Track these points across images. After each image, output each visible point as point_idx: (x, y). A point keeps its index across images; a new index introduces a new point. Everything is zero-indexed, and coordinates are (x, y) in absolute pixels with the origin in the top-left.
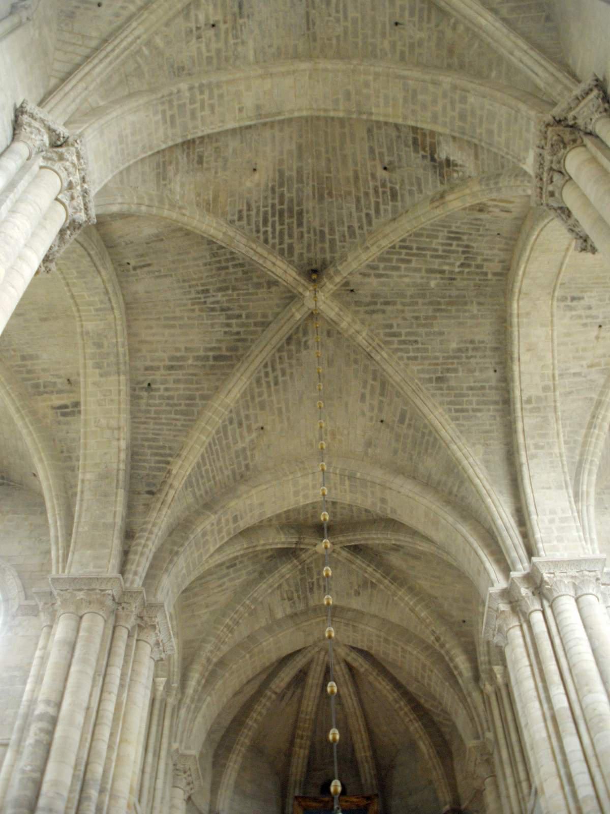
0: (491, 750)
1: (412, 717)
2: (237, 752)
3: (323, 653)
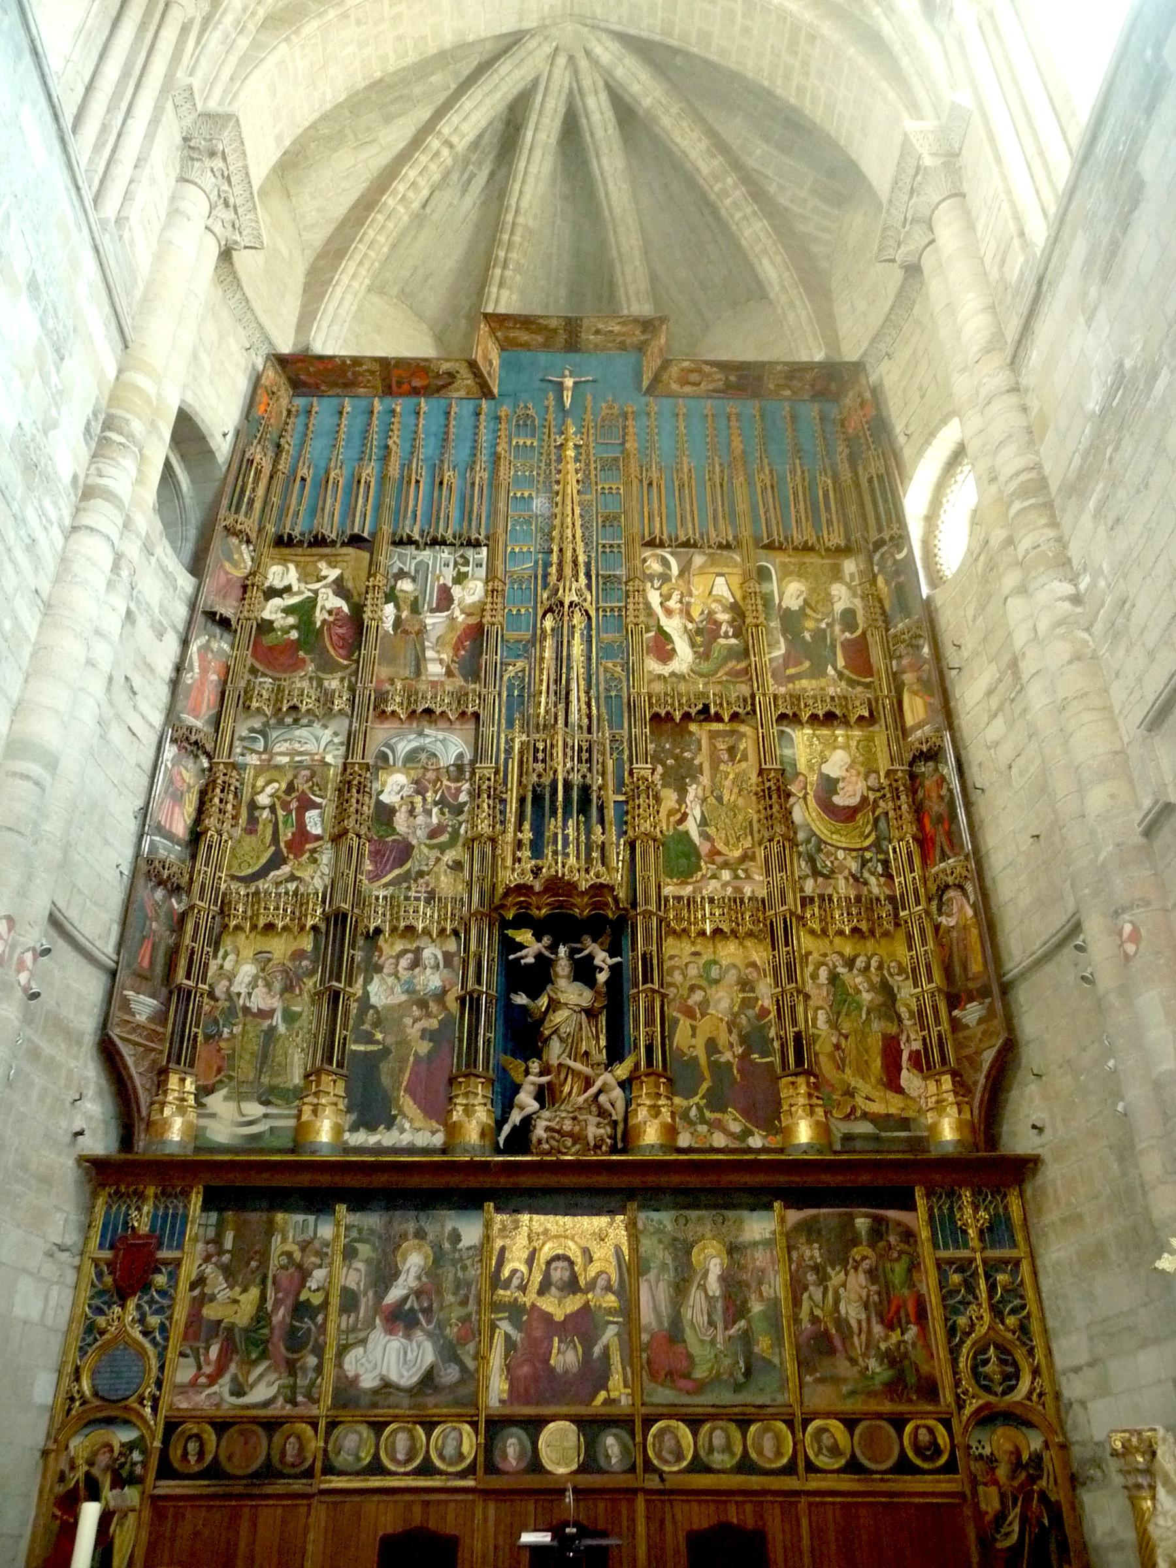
0: (957, 146)
1: (748, 210)
2: (358, 257)
3: (562, 60)
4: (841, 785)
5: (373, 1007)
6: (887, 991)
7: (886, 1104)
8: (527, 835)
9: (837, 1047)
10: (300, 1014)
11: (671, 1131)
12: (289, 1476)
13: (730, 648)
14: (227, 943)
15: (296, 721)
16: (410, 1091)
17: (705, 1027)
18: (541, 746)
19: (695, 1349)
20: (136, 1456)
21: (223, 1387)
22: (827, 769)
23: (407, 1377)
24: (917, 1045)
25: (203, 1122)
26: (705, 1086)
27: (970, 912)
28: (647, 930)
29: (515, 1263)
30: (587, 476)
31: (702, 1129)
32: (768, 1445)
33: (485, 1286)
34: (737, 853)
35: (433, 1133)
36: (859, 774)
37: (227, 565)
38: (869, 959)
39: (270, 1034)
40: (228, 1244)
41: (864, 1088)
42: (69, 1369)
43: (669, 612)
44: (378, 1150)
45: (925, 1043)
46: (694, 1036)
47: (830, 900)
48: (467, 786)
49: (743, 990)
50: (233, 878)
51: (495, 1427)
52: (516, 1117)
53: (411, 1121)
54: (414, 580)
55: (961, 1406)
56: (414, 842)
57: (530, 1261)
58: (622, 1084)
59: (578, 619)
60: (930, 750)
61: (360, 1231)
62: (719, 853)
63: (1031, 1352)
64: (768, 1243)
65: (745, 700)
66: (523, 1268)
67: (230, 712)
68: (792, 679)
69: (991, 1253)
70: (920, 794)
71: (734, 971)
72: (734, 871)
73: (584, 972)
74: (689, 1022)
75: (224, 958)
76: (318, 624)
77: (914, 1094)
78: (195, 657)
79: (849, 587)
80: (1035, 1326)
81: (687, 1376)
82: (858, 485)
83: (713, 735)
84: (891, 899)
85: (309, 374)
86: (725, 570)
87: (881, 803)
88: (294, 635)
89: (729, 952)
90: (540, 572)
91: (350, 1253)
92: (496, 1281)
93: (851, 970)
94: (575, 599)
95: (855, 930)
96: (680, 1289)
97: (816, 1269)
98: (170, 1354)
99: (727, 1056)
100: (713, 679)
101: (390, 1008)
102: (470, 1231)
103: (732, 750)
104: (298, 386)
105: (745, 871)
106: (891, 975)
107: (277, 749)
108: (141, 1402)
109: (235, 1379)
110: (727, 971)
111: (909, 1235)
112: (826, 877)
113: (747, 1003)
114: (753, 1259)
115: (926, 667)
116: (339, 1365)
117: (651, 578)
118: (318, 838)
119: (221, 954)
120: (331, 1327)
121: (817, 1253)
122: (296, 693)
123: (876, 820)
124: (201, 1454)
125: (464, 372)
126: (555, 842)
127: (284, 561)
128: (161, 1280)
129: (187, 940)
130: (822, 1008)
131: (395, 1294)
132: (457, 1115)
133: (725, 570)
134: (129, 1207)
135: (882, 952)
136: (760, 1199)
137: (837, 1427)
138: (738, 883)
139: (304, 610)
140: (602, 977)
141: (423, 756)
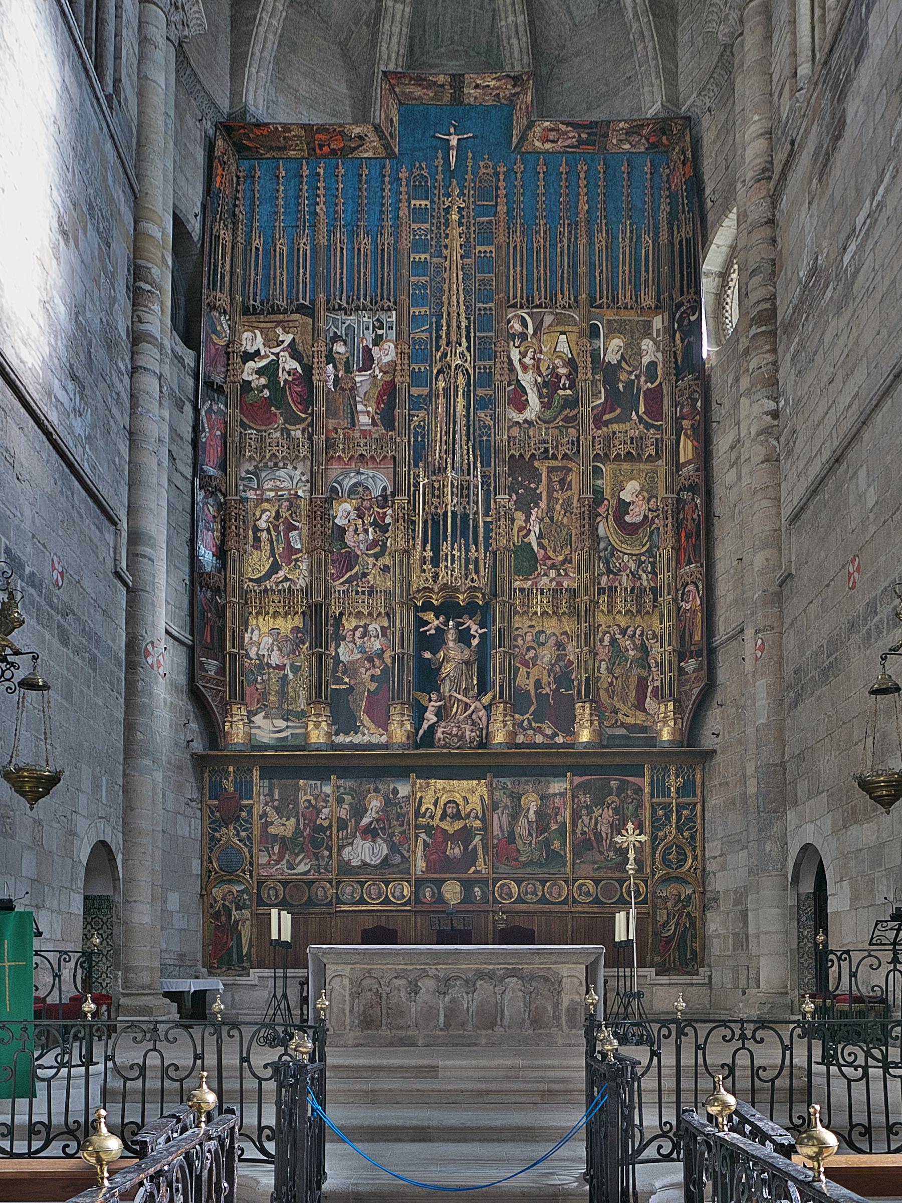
4: (631, 507)
5: (342, 662)
6: (644, 650)
7: (634, 718)
8: (429, 554)
9: (611, 684)
10: (300, 667)
11: (513, 735)
12: (320, 905)
13: (566, 398)
14: (253, 622)
15: (276, 464)
16: (367, 712)
17: (535, 672)
18: (436, 485)
19: (521, 847)
20: (245, 896)
21: (283, 865)
22: (623, 495)
23: (376, 861)
24: (657, 683)
25: (253, 731)
26: (533, 708)
27: (699, 602)
28: (502, 613)
29: (427, 805)
30: (468, 239)
31: (530, 732)
32: (555, 891)
33: (411, 815)
34: (561, 558)
35: (381, 736)
36: (643, 500)
37: (214, 337)
38: (636, 629)
39: (284, 679)
40: (277, 797)
41: (623, 708)
42: (206, 857)
43: (525, 368)
44: (352, 746)
45: (662, 682)
46: (528, 678)
47: (616, 591)
48: (390, 511)
49: (558, 650)
50: (251, 580)
51: (419, 883)
52: (425, 726)
53: (368, 729)
54: (345, 344)
55: (654, 875)
56: (359, 553)
57: (435, 804)
58: (484, 708)
59: (461, 381)
60: (691, 485)
61: (345, 789)
62: (550, 558)
63: (694, 849)
64: (562, 794)
65: (573, 444)
66: (432, 807)
67: (232, 459)
68: (606, 424)
69: (680, 800)
70: (681, 516)
71: (554, 638)
72: (558, 570)
73: (464, 637)
74: (525, 669)
75: (252, 633)
76: (282, 383)
77: (651, 712)
78: (205, 420)
79: (654, 340)
80: (699, 837)
81: (517, 860)
82: (672, 244)
83: (551, 470)
84: (654, 590)
85: (249, 139)
86: (567, 328)
87: (656, 521)
88: (266, 393)
89: (551, 626)
90: (434, 335)
91: (340, 801)
92: (417, 814)
93: (624, 636)
94: (459, 362)
95: (627, 612)
96: (514, 817)
97: (587, 807)
98: (255, 851)
99: (547, 690)
100: (552, 425)
101: (352, 662)
102: (404, 790)
103: (562, 482)
104: (241, 149)
105: (565, 570)
106: (648, 640)
107: (265, 487)
108: (244, 873)
109: (288, 861)
110: (549, 638)
111: (639, 790)
112: (615, 574)
113: (560, 658)
114: (554, 803)
115: (698, 417)
116: (340, 855)
117: (512, 337)
118: (300, 551)
119: (249, 630)
120: (334, 837)
121: (588, 800)
122: (274, 444)
123: (652, 533)
124: (277, 896)
125: (372, 136)
126: (446, 560)
127: (252, 328)
128: (244, 814)
129: (229, 624)
130: (604, 660)
131: (365, 821)
132: (394, 726)
133: (567, 328)
134: (221, 778)
135: (644, 625)
136: (559, 772)
137: (590, 885)
138: (559, 579)
139: (270, 370)
140: (475, 642)
141: (361, 489)
